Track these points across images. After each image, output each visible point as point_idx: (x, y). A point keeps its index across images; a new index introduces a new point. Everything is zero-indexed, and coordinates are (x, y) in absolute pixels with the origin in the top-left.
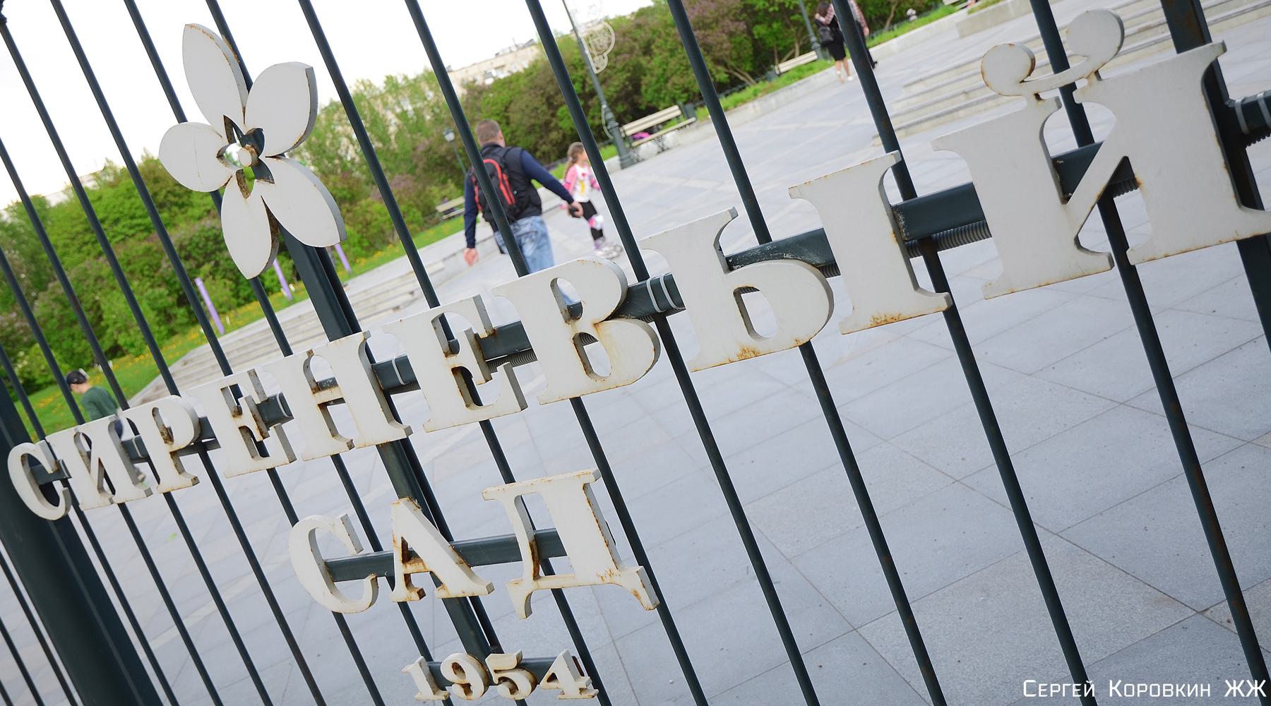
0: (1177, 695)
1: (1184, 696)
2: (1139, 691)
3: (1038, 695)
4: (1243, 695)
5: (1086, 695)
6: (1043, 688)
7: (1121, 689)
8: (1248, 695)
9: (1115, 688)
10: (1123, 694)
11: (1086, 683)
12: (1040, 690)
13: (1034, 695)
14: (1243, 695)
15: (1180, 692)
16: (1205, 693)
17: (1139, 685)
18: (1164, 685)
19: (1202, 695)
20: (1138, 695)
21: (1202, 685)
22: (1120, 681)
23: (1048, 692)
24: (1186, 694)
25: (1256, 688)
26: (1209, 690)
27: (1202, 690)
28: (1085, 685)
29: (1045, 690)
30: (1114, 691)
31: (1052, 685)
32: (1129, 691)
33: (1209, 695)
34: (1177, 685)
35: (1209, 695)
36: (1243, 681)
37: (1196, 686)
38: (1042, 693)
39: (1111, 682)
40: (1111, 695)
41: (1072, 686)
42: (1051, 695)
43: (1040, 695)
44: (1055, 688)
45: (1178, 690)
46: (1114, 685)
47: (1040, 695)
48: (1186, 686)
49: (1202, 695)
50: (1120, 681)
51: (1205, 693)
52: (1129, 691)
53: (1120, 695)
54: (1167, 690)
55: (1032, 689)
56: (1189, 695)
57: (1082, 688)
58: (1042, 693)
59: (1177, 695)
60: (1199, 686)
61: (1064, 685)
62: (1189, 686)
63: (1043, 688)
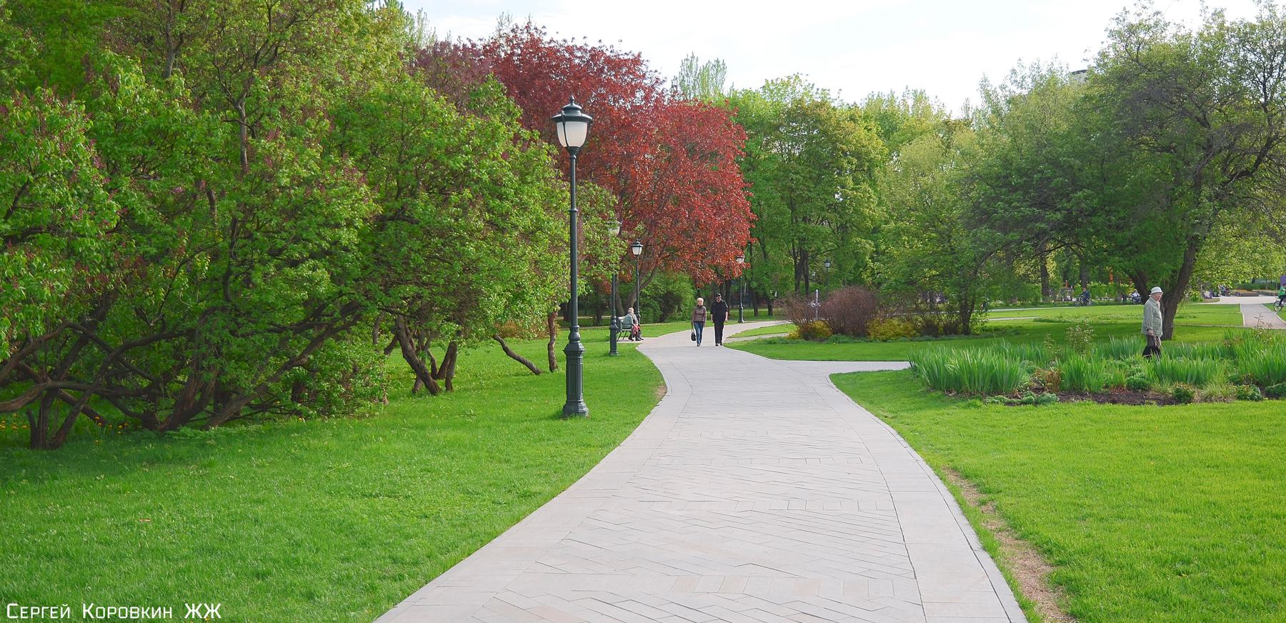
1: (149, 617)
2: (109, 613)
3: (19, 614)
5: (62, 616)
6: (24, 610)
7: (93, 611)
9: (88, 611)
10: (94, 615)
12: (22, 612)
13: (16, 617)
17: (109, 608)
20: (109, 617)
22: (92, 605)
23: (29, 614)
24: (151, 616)
25: (212, 611)
26: (170, 612)
27: (165, 612)
28: (62, 608)
30: (87, 614)
31: (32, 608)
32: (101, 613)
36: (200, 605)
37: (159, 609)
38: (24, 615)
41: (50, 609)
42: (32, 617)
43: (22, 617)
45: (143, 612)
46: (87, 609)
47: (22, 617)
50: (92, 605)
52: (101, 613)
53: (92, 617)
54: (135, 612)
56: (153, 617)
58: (24, 615)
60: (162, 611)
61: (43, 608)
63: (24, 610)
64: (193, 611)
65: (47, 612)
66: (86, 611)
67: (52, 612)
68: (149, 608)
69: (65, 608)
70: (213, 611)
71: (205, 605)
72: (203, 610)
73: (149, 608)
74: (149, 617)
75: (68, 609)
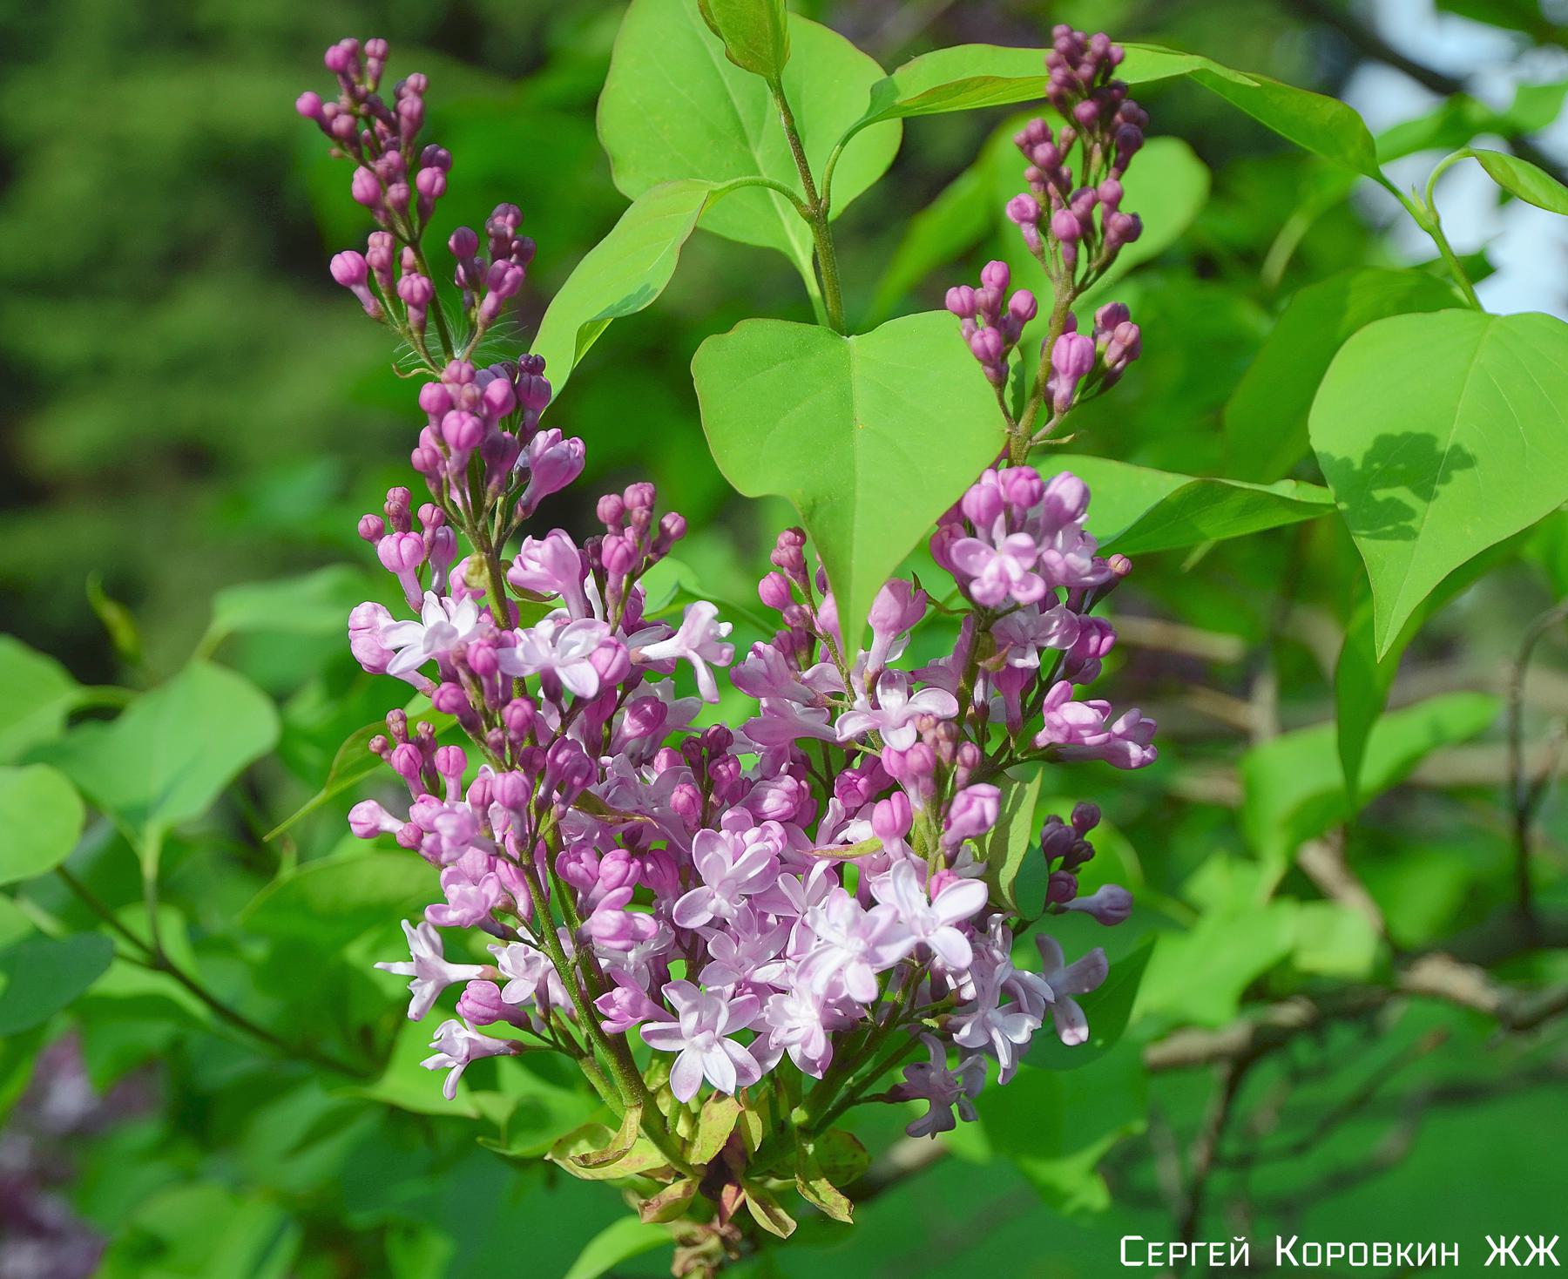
0: (1399, 1264)
1: (1412, 1264)
2: (1329, 1256)
4: (1517, 1263)
5: (1233, 1262)
6: (1155, 1249)
7: (1296, 1251)
8: (1527, 1263)
9: (1287, 1250)
10: (1299, 1258)
11: (1235, 1242)
12: (1151, 1254)
13: (1139, 1264)
14: (1517, 1263)
15: (1403, 1258)
16: (1450, 1259)
18: (1375, 1245)
19: (1443, 1264)
20: (1329, 1264)
21: (1443, 1245)
22: (1295, 1238)
23: (1165, 1258)
24: (1415, 1261)
26: (1456, 1254)
27: (1444, 1254)
28: (1232, 1245)
29: (1159, 1254)
30: (1284, 1255)
31: (1172, 1245)
33: (1456, 1264)
34: (1399, 1245)
35: (1456, 1264)
36: (1517, 1238)
37: (1433, 1246)
38: (1155, 1259)
39: (1279, 1239)
40: (1279, 1263)
41: (1208, 1246)
42: (1171, 1264)
43: (1151, 1264)
44: (1336, 1250)
45: (1399, 1254)
46: (1284, 1246)
47: (1151, 1264)
48: (1414, 1249)
49: (1443, 1264)
50: (1295, 1238)
51: (1450, 1259)
52: (1312, 1254)
53: (1295, 1263)
55: (1136, 1251)
56: (1420, 1262)
57: (1226, 1249)
58: (1155, 1259)
59: (1399, 1264)
61: (1194, 1245)
62: (1420, 1245)
63: (1155, 1249)
64: (1502, 1250)
65: (1202, 1253)
66: (1282, 1250)
67: (1212, 1254)
68: (1411, 1245)
69: (1238, 1246)
70: (1543, 1250)
71: (1527, 1238)
72: (1523, 1251)
73: (1411, 1245)
74: (1412, 1264)
75: (1246, 1247)
